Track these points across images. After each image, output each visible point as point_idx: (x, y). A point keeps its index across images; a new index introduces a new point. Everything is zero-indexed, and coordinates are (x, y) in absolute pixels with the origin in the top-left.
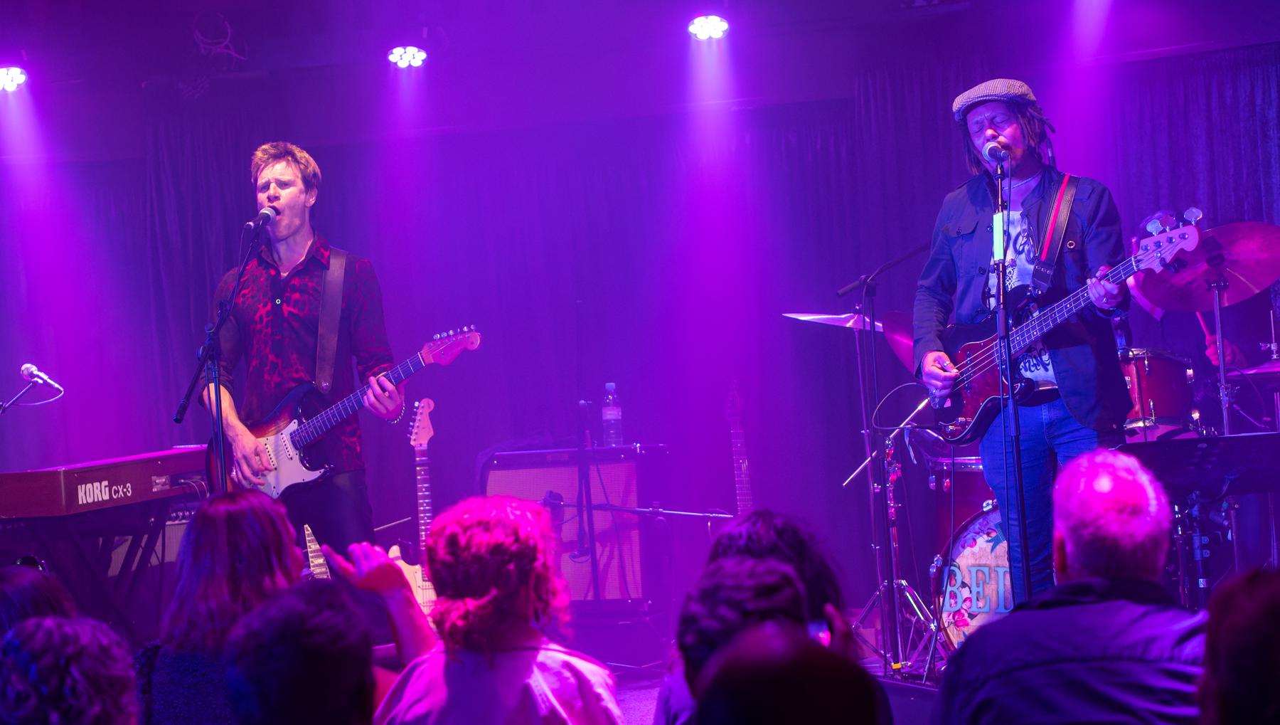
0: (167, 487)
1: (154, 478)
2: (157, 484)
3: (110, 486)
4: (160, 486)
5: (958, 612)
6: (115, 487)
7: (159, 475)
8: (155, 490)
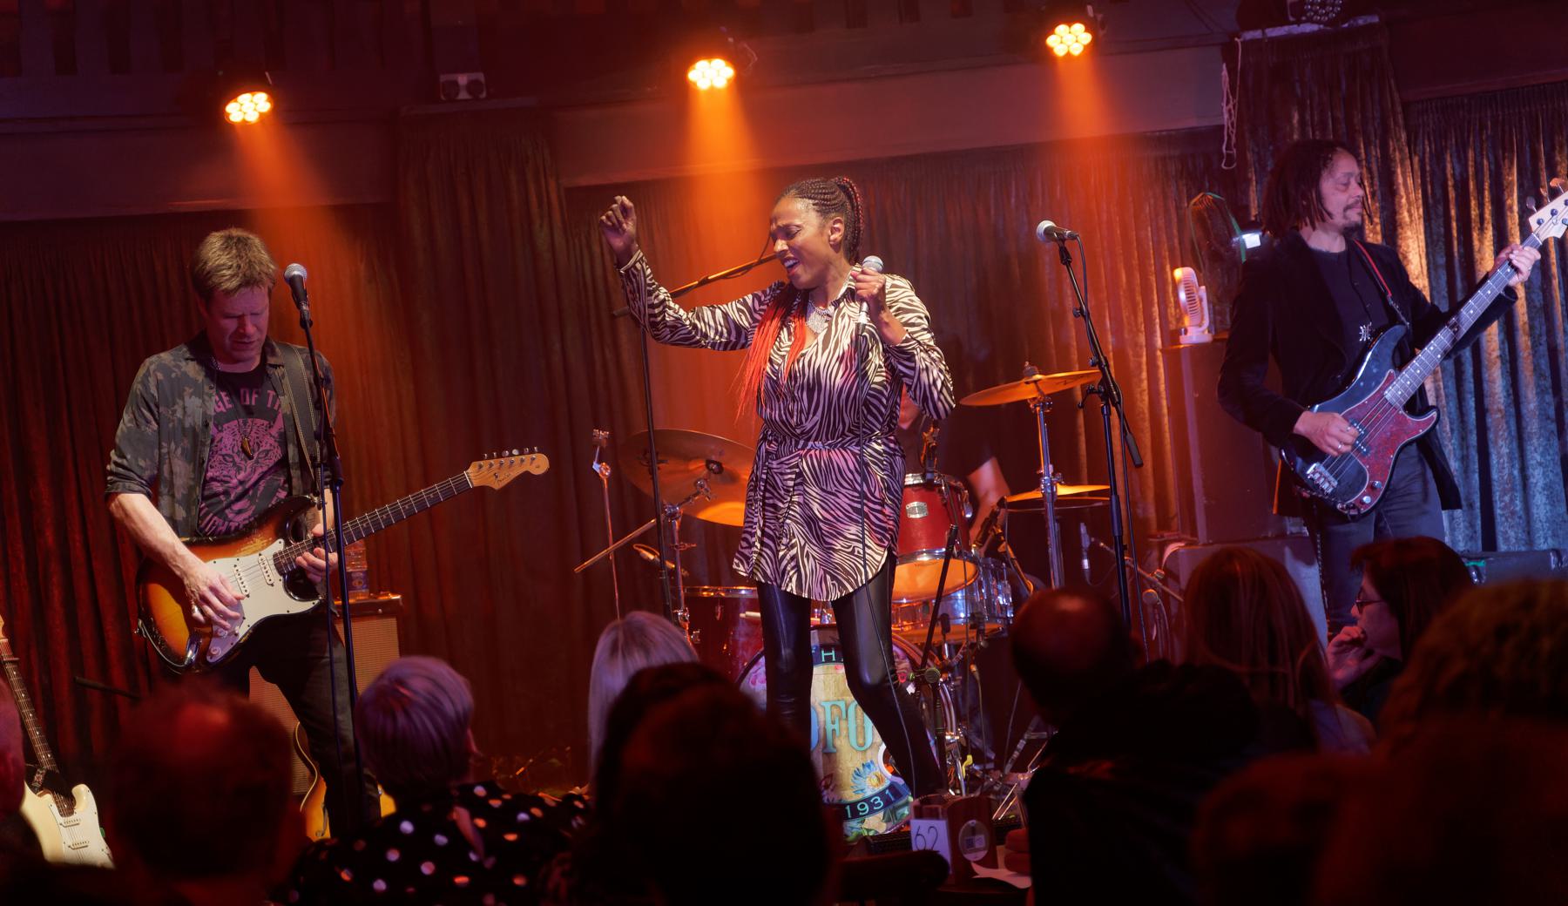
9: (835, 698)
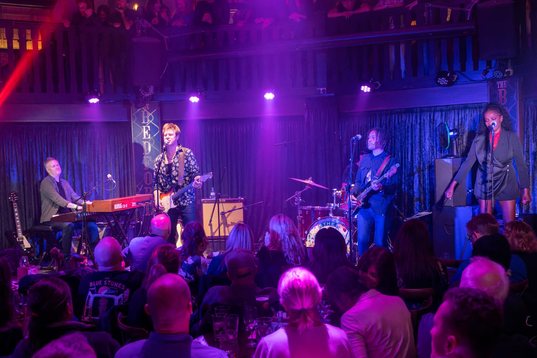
0: (136, 205)
1: (133, 203)
3: (122, 205)
5: (311, 245)
6: (123, 205)
7: (134, 202)
8: (133, 206)
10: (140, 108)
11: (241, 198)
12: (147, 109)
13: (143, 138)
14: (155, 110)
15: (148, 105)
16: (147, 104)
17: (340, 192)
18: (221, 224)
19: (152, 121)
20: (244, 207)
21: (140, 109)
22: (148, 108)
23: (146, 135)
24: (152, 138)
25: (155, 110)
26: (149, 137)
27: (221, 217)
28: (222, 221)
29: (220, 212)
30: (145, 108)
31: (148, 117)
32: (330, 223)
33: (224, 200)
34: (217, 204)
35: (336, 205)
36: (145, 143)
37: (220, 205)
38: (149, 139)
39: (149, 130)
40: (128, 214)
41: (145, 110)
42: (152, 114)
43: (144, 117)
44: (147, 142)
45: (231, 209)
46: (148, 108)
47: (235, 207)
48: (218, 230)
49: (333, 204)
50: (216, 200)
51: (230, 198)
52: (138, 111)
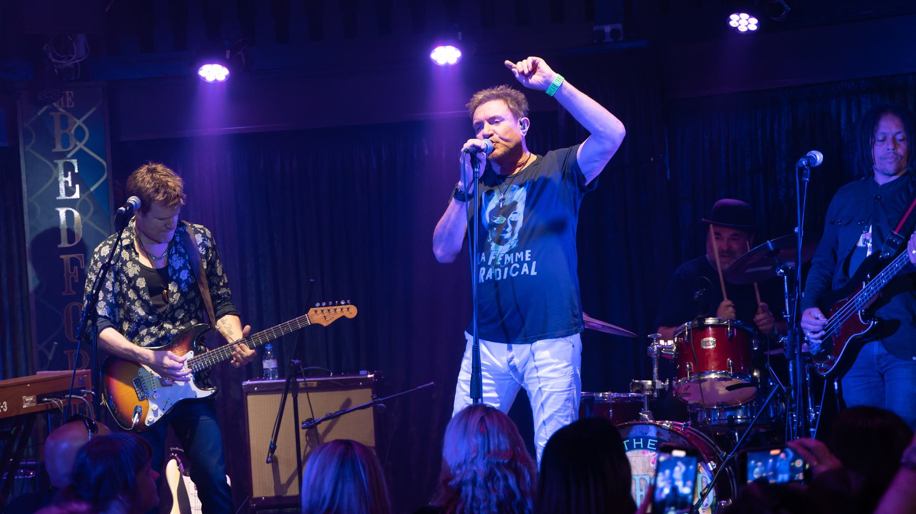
0: (34, 404)
1: (24, 397)
2: (27, 402)
4: (27, 404)
7: (28, 395)
8: (24, 406)
9: (643, 473)
10: (44, 106)
11: (367, 374)
12: (68, 106)
13: (58, 198)
14: (93, 110)
15: (70, 94)
16: (67, 93)
17: (670, 342)
18: (306, 457)
19: (86, 145)
20: (375, 403)
21: (45, 108)
22: (71, 104)
23: (67, 188)
24: (85, 196)
25: (93, 110)
26: (77, 195)
27: (307, 435)
28: (309, 449)
29: (302, 418)
30: (60, 105)
31: (70, 131)
32: (641, 443)
33: (313, 381)
34: (290, 397)
35: (659, 385)
36: (62, 212)
37: (302, 397)
38: (77, 199)
39: (76, 171)
40: (12, 432)
41: (61, 110)
42: (84, 122)
43: (58, 132)
44: (71, 209)
45: (335, 408)
46: (71, 104)
47: (348, 402)
48: (296, 479)
49: (649, 382)
50: (288, 381)
51: (334, 375)
52: (39, 114)
